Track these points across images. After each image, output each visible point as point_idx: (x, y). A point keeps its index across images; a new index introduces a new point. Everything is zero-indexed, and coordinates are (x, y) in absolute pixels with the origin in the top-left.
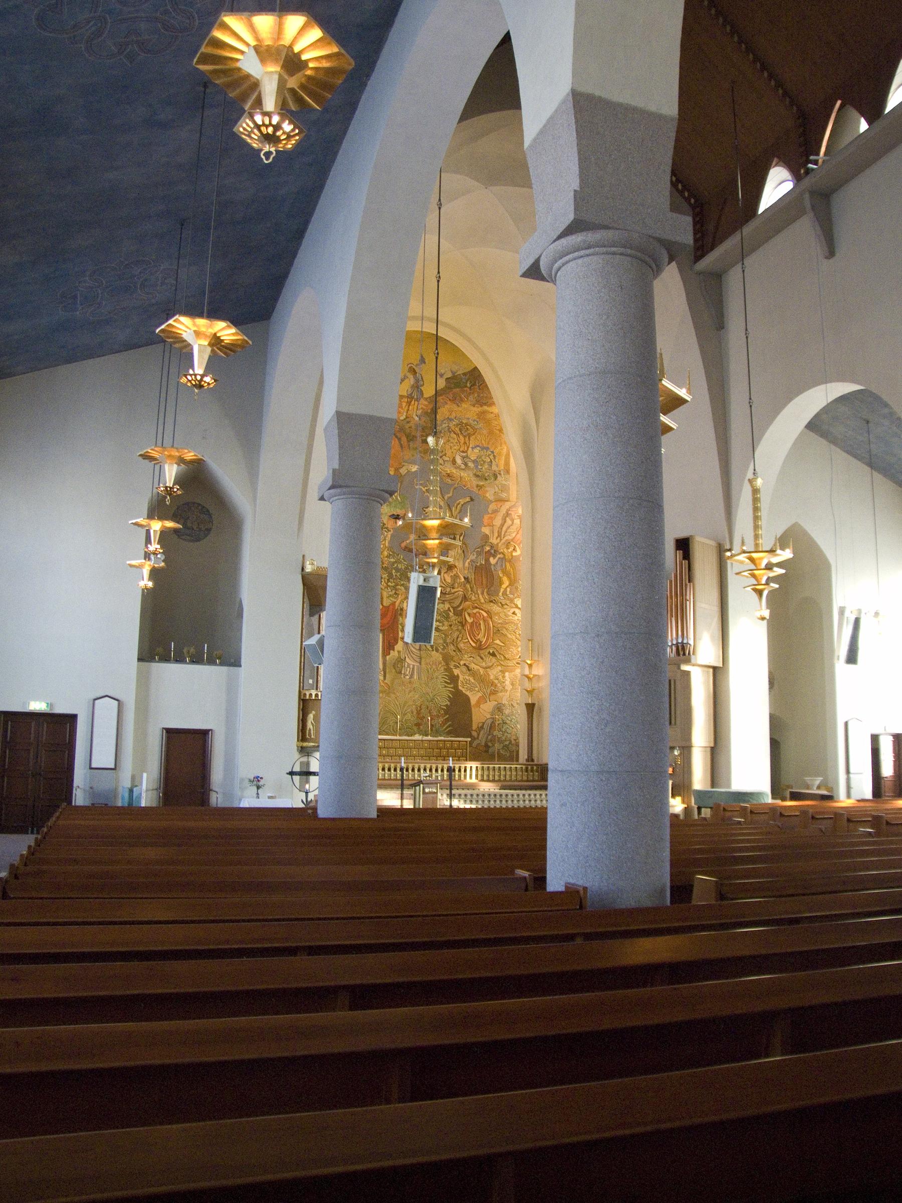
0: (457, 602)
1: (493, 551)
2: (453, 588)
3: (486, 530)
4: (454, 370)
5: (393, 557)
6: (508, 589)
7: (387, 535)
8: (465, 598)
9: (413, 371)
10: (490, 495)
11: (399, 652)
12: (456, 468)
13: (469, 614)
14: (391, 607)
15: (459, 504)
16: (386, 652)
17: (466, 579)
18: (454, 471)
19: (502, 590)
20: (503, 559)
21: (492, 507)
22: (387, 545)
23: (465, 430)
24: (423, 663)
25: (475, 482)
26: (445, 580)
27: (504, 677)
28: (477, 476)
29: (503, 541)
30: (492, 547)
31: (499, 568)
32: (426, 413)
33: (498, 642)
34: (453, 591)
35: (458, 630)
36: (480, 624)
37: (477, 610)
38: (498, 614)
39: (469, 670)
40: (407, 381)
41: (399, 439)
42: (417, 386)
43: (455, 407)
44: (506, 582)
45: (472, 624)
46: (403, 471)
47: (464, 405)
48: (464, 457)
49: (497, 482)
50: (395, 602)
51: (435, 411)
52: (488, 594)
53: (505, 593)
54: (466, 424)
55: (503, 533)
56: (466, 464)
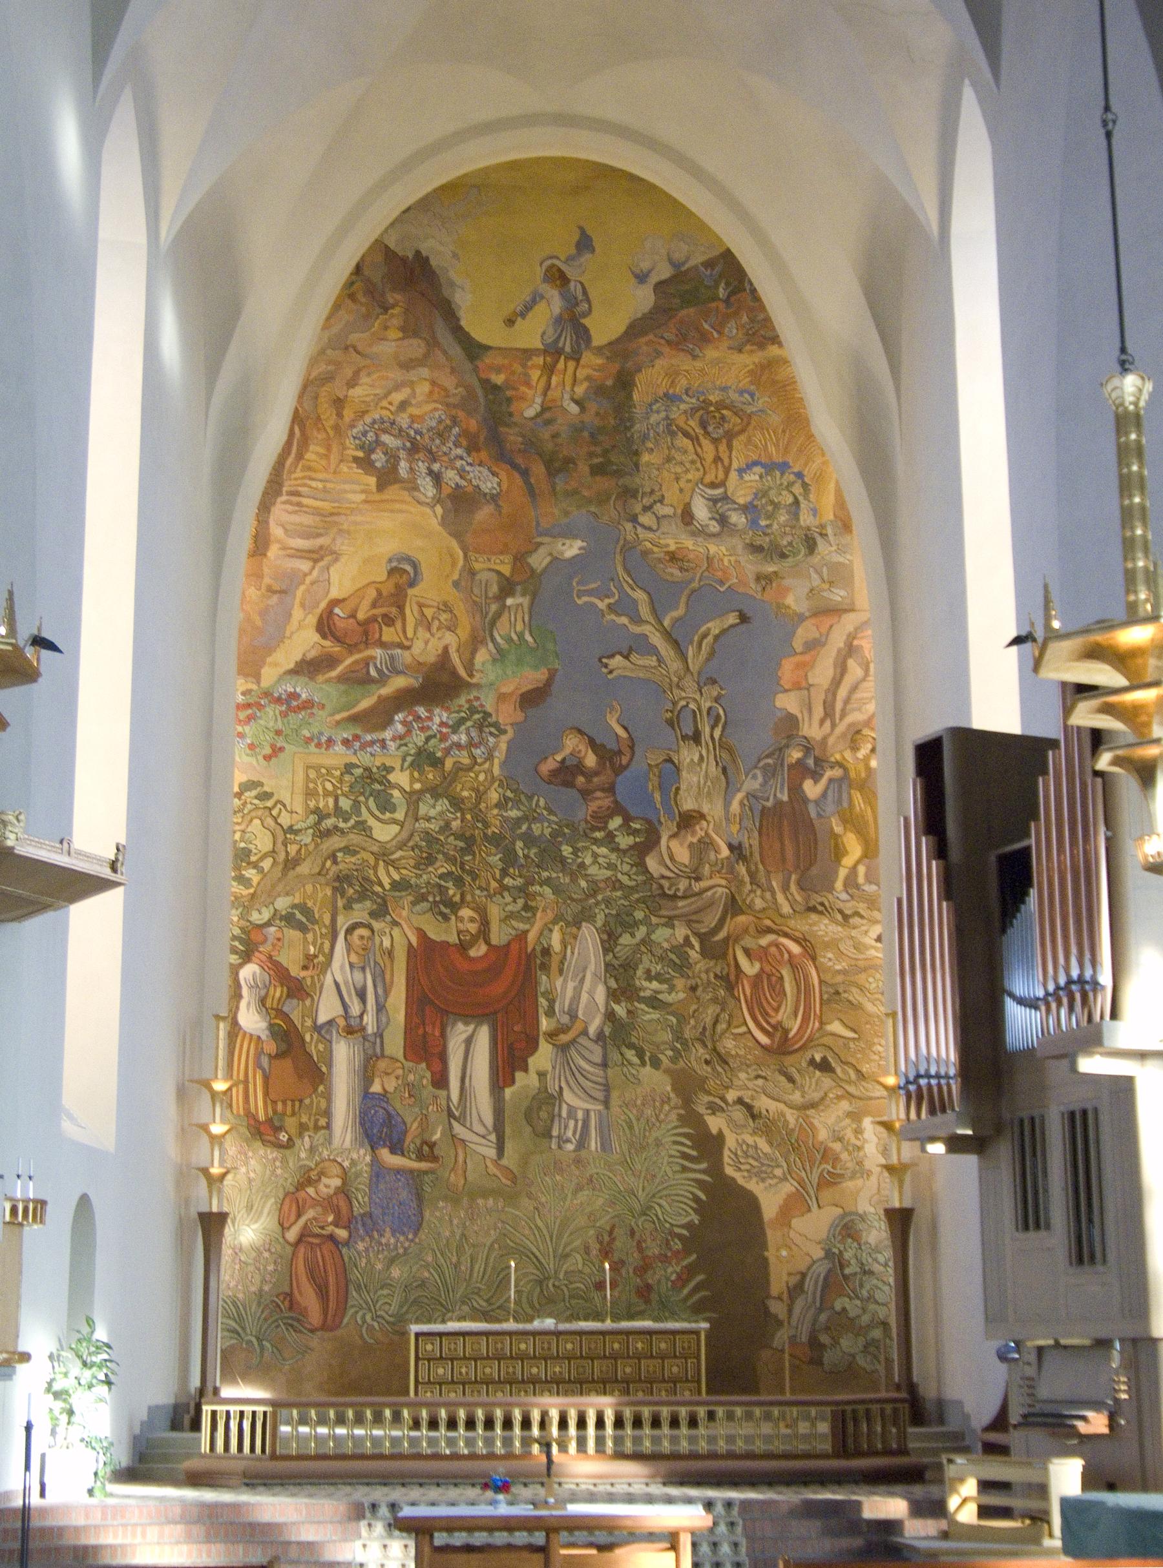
0: (710, 920)
1: (810, 762)
2: (698, 879)
3: (788, 702)
4: (678, 256)
5: (517, 803)
6: (861, 870)
7: (496, 745)
8: (734, 906)
9: (557, 277)
10: (795, 600)
11: (542, 1075)
12: (693, 534)
13: (747, 952)
14: (515, 947)
15: (705, 636)
18: (689, 543)
19: (843, 873)
20: (844, 781)
21: (804, 633)
22: (496, 771)
24: (615, 1100)
25: (750, 565)
26: (672, 858)
27: (858, 1131)
28: (756, 549)
29: (841, 728)
30: (808, 750)
31: (830, 808)
32: (599, 390)
33: (836, 1027)
34: (697, 887)
35: (715, 1000)
36: (781, 978)
37: (771, 937)
38: (833, 944)
39: (754, 1117)
40: (541, 308)
41: (525, 473)
43: (684, 362)
44: (854, 849)
45: (757, 981)
46: (539, 561)
47: (711, 353)
48: (715, 501)
49: (815, 559)
50: (528, 931)
51: (625, 382)
52: (801, 888)
53: (851, 882)
54: (720, 405)
55: (839, 705)
56: (723, 520)
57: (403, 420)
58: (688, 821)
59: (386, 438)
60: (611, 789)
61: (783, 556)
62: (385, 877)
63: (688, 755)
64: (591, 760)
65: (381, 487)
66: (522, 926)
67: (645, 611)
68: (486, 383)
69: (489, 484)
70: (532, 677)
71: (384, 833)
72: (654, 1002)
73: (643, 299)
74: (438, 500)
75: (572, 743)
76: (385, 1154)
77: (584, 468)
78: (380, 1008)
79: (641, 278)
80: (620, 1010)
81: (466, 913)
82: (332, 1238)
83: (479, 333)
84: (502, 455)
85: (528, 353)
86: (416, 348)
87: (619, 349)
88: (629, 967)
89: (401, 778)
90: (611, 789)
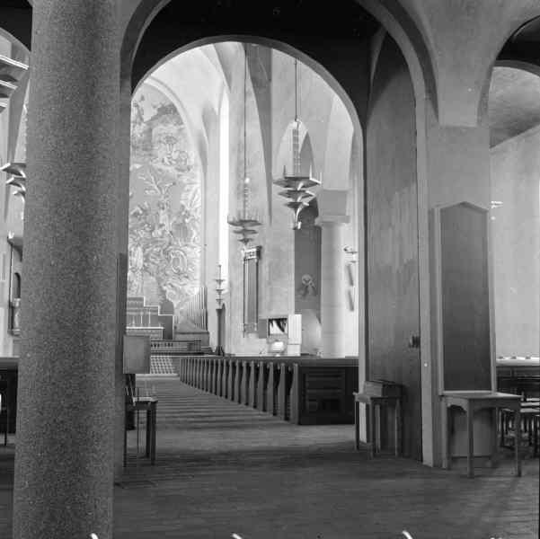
0: (165, 247)
3: (183, 202)
8: (170, 244)
10: (185, 181)
17: (171, 232)
20: (194, 219)
21: (186, 188)
25: (176, 173)
32: (144, 132)
33: (190, 269)
38: (190, 253)
43: (161, 126)
44: (195, 233)
51: (151, 130)
58: (161, 226)
60: (145, 218)
61: (183, 171)
63: (162, 212)
64: (141, 212)
72: (153, 263)
73: (155, 112)
75: (137, 209)
79: (155, 107)
80: (146, 264)
87: (149, 123)
90: (145, 218)
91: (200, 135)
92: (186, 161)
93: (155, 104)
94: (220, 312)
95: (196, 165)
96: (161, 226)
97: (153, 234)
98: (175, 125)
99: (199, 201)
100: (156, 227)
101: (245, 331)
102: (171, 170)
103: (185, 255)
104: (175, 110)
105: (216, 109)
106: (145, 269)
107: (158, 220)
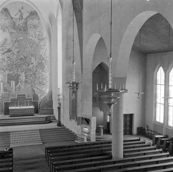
0: (34, 72)
3: (41, 53)
4: (32, 10)
12: (33, 37)
16: (15, 86)
17: (36, 66)
21: (43, 47)
23: (35, 27)
25: (38, 41)
28: (38, 39)
29: (46, 56)
30: (43, 58)
40: (18, 14)
42: (21, 16)
44: (46, 66)
46: (18, 39)
49: (44, 41)
51: (26, 22)
53: (46, 69)
54: (35, 25)
56: (35, 36)
57: (5, 25)
58: (32, 63)
59: (4, 27)
60: (25, 60)
62: (5, 68)
63: (32, 57)
64: (23, 58)
65: (3, 31)
66: (17, 72)
67: (28, 45)
68: (13, 21)
69: (14, 31)
70: (18, 50)
71: (5, 64)
73: (28, 14)
74: (9, 33)
76: (5, 92)
77: (23, 30)
78: (5, 80)
80: (26, 79)
81: (12, 71)
82: (1, 99)
83: (13, 17)
84: (15, 29)
85: (17, 19)
86: (6, 17)
88: (27, 76)
89: (6, 59)
91: (49, 27)
92: (42, 36)
93: (28, 11)
94: (59, 108)
95: (46, 38)
96: (32, 63)
97: (29, 67)
98: (37, 20)
99: (48, 53)
100: (30, 64)
101: (70, 118)
102: (36, 40)
103: (43, 75)
104: (37, 14)
105: (56, 16)
106: (26, 82)
107: (31, 60)
